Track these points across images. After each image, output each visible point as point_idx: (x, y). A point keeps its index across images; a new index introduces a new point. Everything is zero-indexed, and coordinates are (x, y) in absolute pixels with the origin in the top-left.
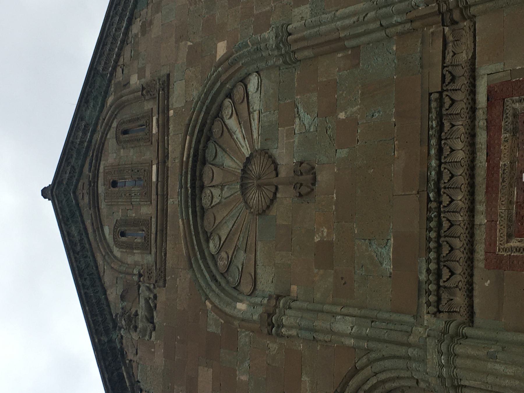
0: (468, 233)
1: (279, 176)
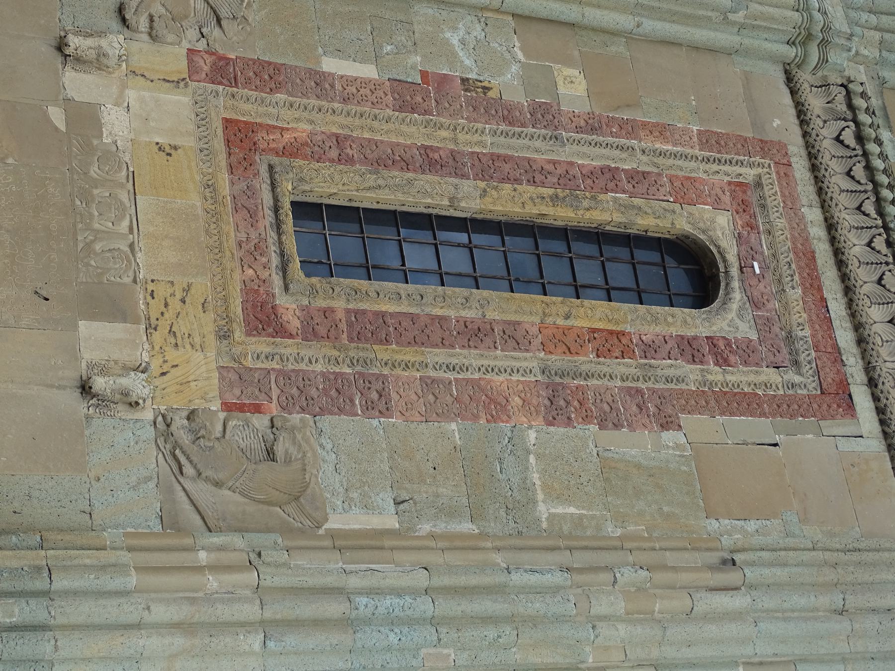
0: (826, 193)
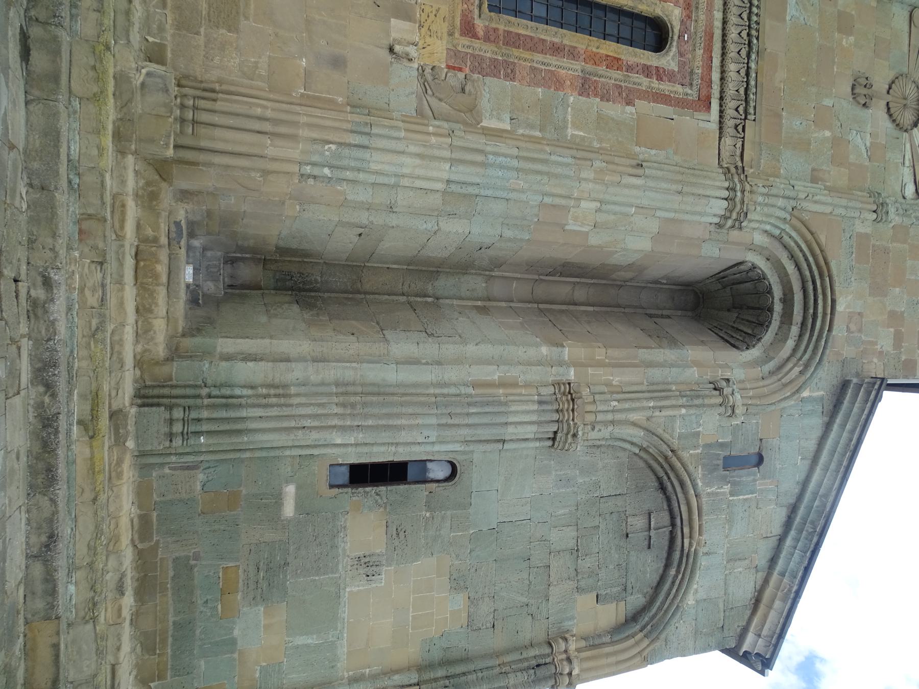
1: (885, 103)
